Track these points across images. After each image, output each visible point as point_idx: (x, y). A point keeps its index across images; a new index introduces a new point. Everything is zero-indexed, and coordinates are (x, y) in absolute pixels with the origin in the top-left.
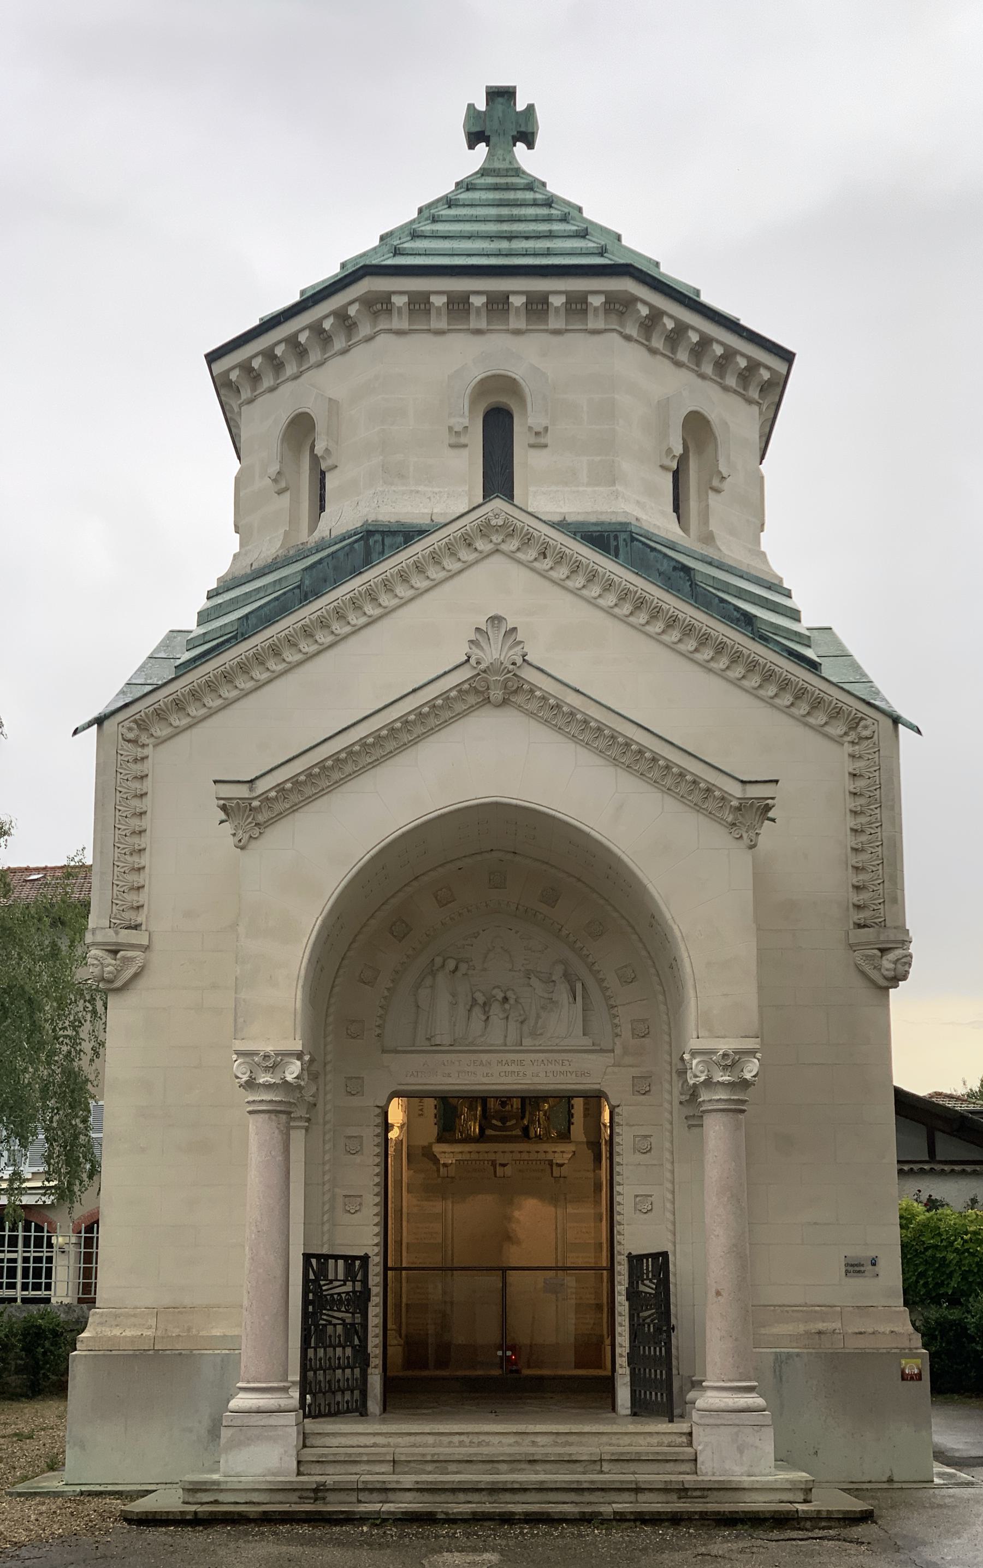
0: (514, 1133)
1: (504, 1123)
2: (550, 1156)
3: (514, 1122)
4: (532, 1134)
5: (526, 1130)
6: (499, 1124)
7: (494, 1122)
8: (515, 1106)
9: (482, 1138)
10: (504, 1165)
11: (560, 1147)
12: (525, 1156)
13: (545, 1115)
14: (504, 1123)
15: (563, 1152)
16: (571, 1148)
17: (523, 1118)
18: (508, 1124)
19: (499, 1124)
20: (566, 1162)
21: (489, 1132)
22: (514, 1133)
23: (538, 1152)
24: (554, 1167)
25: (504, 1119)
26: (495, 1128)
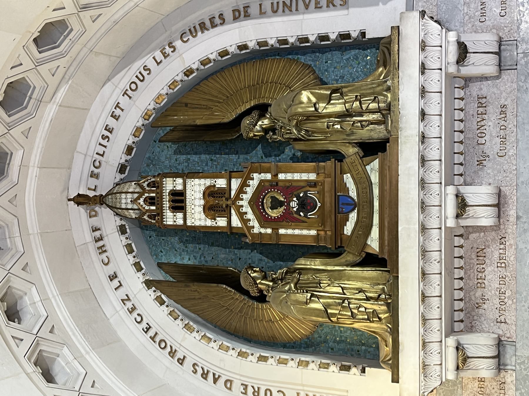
0: (375, 178)
1: (353, 205)
2: (435, 82)
3: (348, 179)
4: (377, 133)
5: (375, 148)
6: (353, 216)
7: (348, 229)
8: (312, 176)
9: (384, 261)
10: (462, 206)
11: (409, 56)
12: (436, 150)
13: (329, 100)
14: (353, 205)
15: (423, 46)
16: (412, 30)
17: (339, 157)
18: (353, 193)
19: (353, 216)
20: (452, 36)
21: (374, 243)
22: (375, 178)
23: (423, 114)
24: (465, 71)
25: (341, 205)
26: (363, 227)
